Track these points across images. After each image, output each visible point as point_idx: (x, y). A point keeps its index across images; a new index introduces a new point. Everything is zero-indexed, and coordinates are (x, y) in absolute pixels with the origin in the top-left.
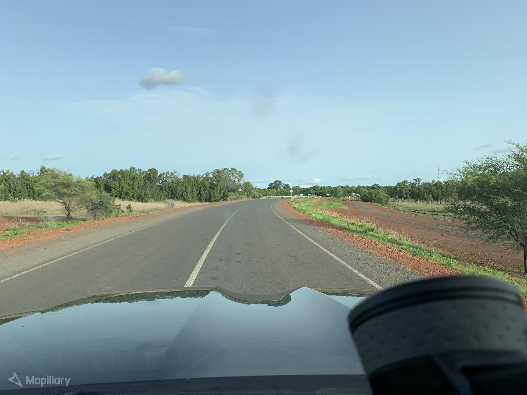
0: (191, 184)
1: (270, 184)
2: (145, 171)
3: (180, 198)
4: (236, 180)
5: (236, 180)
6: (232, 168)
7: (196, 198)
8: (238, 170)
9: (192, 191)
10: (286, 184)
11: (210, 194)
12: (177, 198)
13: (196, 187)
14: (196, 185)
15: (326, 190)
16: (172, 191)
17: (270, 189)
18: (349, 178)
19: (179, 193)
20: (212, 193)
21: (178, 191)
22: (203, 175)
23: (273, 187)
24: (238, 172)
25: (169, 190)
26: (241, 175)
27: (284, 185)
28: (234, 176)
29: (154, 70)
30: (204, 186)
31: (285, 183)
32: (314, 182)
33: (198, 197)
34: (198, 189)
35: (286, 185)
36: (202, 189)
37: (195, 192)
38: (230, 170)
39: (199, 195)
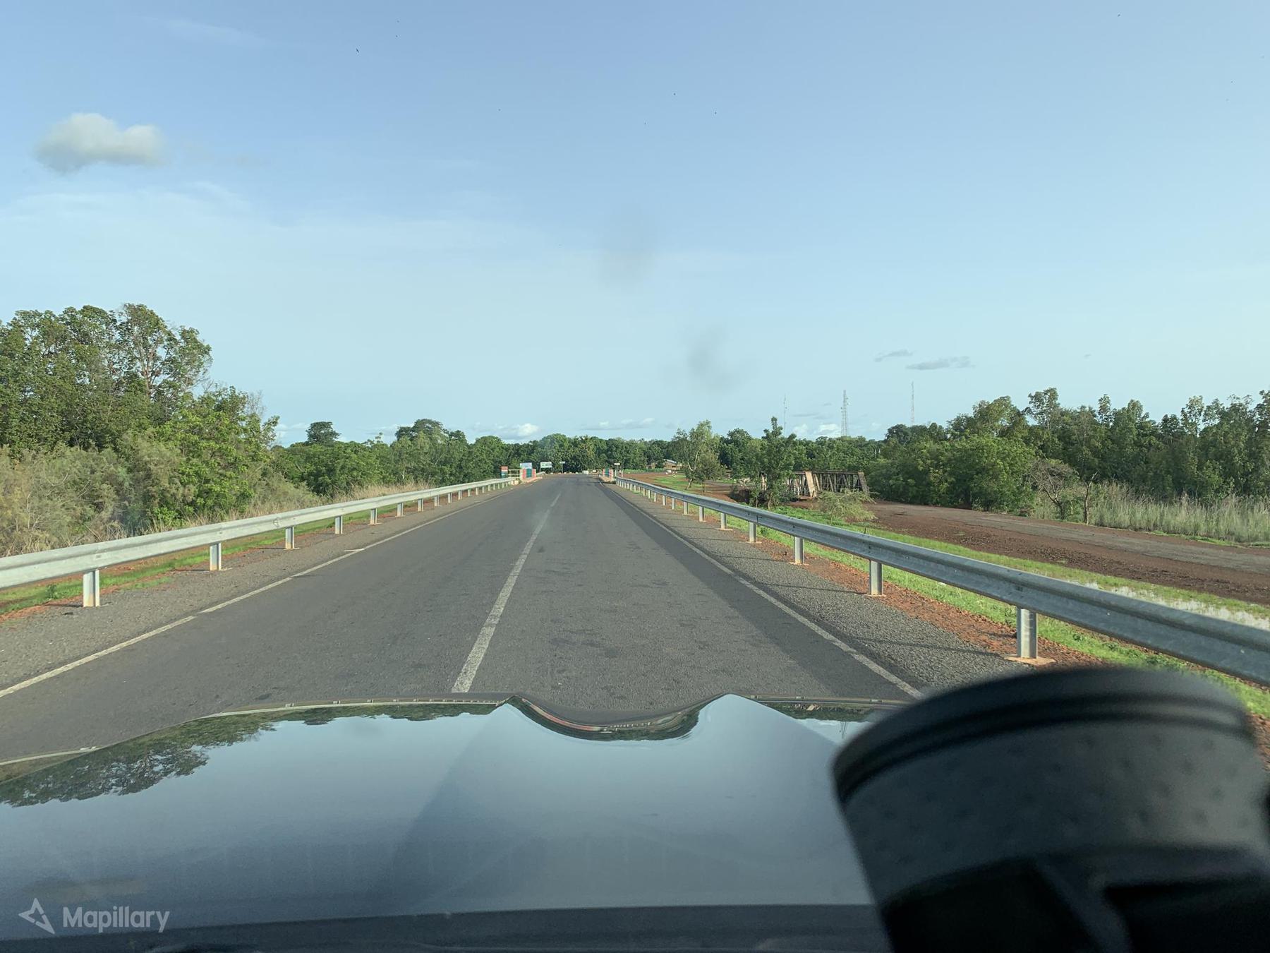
10: (454, 431)
27: (447, 433)
31: (450, 424)
32: (520, 434)
35: (452, 434)
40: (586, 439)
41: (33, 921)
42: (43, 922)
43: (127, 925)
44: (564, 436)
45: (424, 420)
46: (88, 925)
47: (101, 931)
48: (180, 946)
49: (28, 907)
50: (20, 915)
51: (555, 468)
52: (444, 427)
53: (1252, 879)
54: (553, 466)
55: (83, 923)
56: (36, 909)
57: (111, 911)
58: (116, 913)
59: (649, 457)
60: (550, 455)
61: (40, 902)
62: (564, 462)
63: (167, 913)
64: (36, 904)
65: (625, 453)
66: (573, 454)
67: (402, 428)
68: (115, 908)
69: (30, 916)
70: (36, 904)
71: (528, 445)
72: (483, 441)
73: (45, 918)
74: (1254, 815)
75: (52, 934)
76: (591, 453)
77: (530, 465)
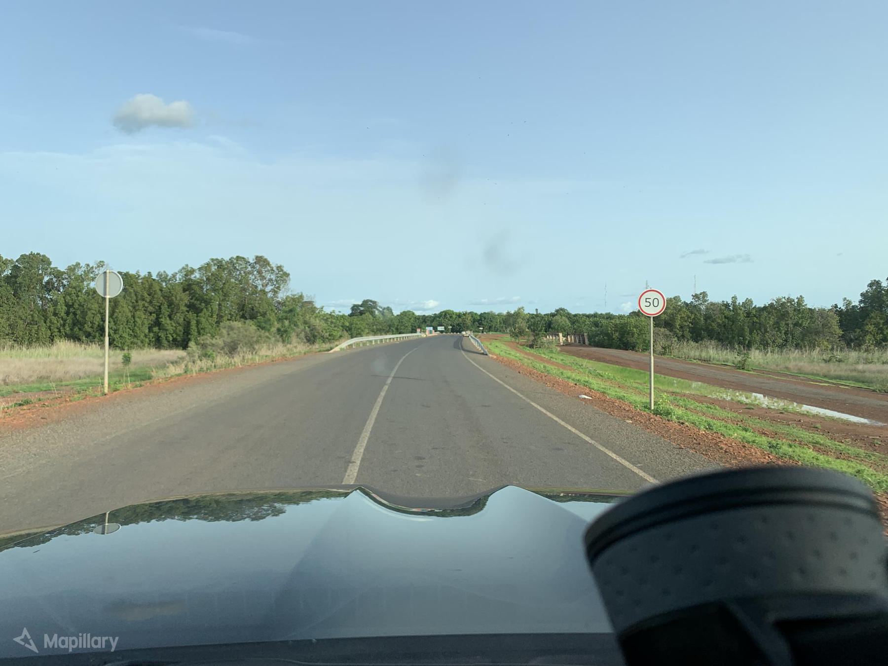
0: (133, 295)
1: (355, 306)
2: (9, 259)
3: (94, 337)
4: (269, 288)
5: (269, 288)
6: (257, 257)
7: (146, 336)
8: (274, 263)
9: (134, 317)
10: (386, 306)
11: (188, 324)
12: (88, 335)
13: (146, 305)
14: (148, 300)
15: (469, 318)
16: (75, 314)
17: (353, 316)
18: (483, 300)
19: (92, 323)
20: (193, 323)
21: (89, 314)
22: (177, 273)
23: (360, 312)
24: (275, 269)
25: (68, 313)
26: (283, 276)
27: (381, 308)
28: (263, 278)
29: (140, 98)
30: (170, 304)
31: (382, 303)
33: (152, 335)
34: (154, 310)
35: (384, 309)
36: (163, 310)
37: (144, 320)
38: (251, 261)
39: (156, 329)
41: (22, 643)
42: (31, 645)
45: (367, 300)
46: (62, 647)
47: (70, 650)
48: (126, 662)
49: (20, 635)
50: (14, 639)
52: (380, 305)
53: (879, 615)
56: (25, 635)
61: (28, 631)
63: (117, 638)
64: (25, 632)
67: (354, 305)
68: (80, 634)
69: (21, 640)
70: (25, 632)
71: (431, 316)
72: (404, 314)
73: (31, 641)
74: (880, 570)
75: (36, 653)
77: (431, 328)
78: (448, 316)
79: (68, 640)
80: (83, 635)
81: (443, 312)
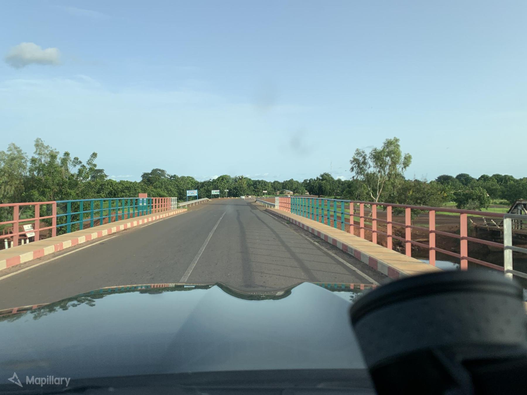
40: (242, 178)
41: (13, 381)
43: (53, 383)
44: (229, 176)
51: (222, 194)
54: (221, 192)
55: (34, 382)
56: (15, 377)
57: (46, 378)
58: (48, 378)
59: (275, 189)
60: (220, 186)
61: (17, 374)
62: (228, 190)
64: (15, 375)
65: (263, 186)
66: (234, 186)
69: (12, 379)
70: (15, 375)
73: (18, 380)
76: (245, 186)
78: (225, 181)
79: (40, 379)
80: (49, 377)
81: (220, 177)
